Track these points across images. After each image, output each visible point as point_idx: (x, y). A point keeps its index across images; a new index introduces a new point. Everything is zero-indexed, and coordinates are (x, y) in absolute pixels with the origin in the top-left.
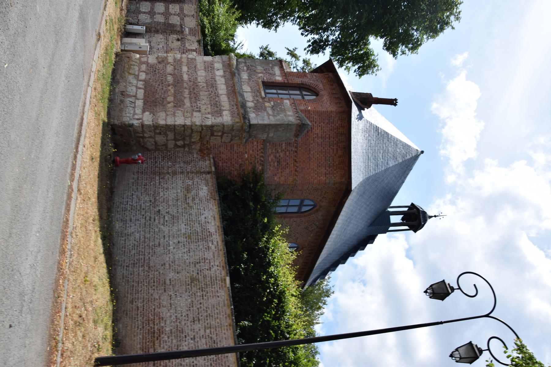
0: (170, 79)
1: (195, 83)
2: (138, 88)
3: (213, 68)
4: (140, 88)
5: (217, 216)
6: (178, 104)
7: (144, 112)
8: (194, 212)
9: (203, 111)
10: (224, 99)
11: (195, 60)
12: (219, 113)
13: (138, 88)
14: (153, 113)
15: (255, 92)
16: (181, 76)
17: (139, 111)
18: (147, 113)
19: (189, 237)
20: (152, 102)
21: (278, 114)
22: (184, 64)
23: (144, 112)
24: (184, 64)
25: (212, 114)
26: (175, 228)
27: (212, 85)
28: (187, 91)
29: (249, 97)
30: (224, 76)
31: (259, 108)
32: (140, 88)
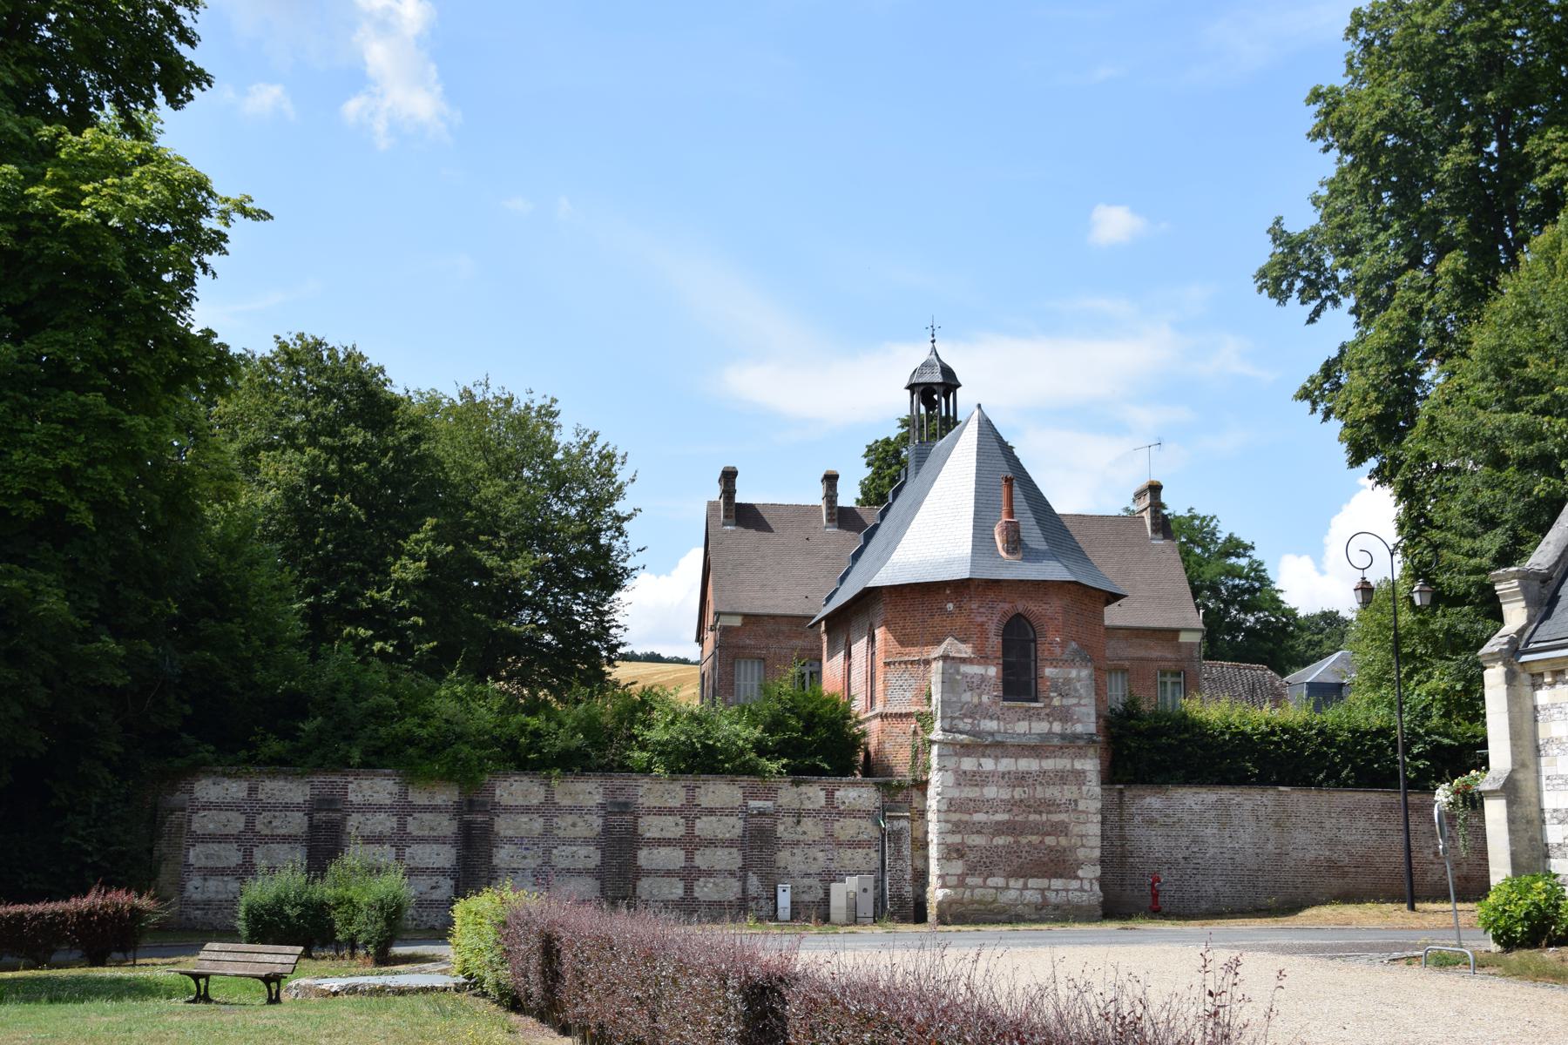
0: (1000, 841)
1: (1011, 805)
2: (1025, 887)
3: (974, 774)
4: (1025, 885)
5: (1195, 790)
6: (1061, 829)
7: (1077, 877)
8: (1187, 818)
9: (1075, 796)
10: (1049, 764)
11: (951, 800)
12: (1079, 777)
13: (1025, 887)
14: (1079, 865)
15: (1029, 716)
16: (997, 823)
17: (1075, 884)
18: (1080, 873)
19: (1222, 826)
20: (1059, 865)
21: (1076, 690)
22: (966, 817)
23: (1077, 877)
24: (966, 817)
25: (1081, 784)
26: (1211, 840)
27: (1021, 779)
28: (1032, 817)
29: (1041, 727)
30: (996, 757)
31: (1064, 715)
32: (1025, 885)
